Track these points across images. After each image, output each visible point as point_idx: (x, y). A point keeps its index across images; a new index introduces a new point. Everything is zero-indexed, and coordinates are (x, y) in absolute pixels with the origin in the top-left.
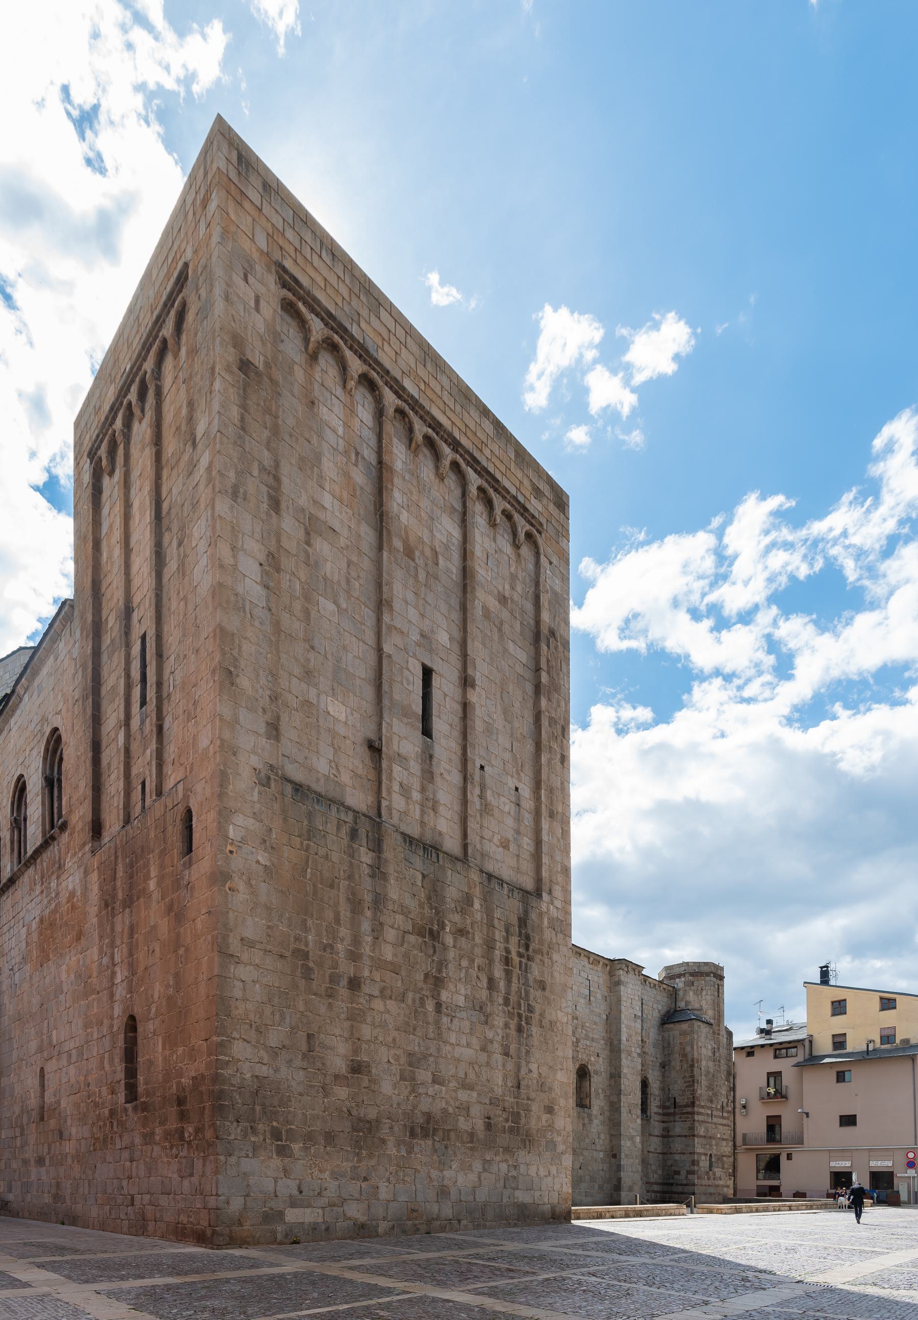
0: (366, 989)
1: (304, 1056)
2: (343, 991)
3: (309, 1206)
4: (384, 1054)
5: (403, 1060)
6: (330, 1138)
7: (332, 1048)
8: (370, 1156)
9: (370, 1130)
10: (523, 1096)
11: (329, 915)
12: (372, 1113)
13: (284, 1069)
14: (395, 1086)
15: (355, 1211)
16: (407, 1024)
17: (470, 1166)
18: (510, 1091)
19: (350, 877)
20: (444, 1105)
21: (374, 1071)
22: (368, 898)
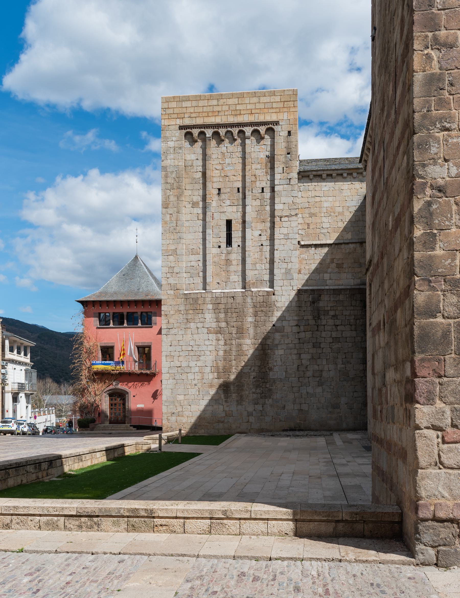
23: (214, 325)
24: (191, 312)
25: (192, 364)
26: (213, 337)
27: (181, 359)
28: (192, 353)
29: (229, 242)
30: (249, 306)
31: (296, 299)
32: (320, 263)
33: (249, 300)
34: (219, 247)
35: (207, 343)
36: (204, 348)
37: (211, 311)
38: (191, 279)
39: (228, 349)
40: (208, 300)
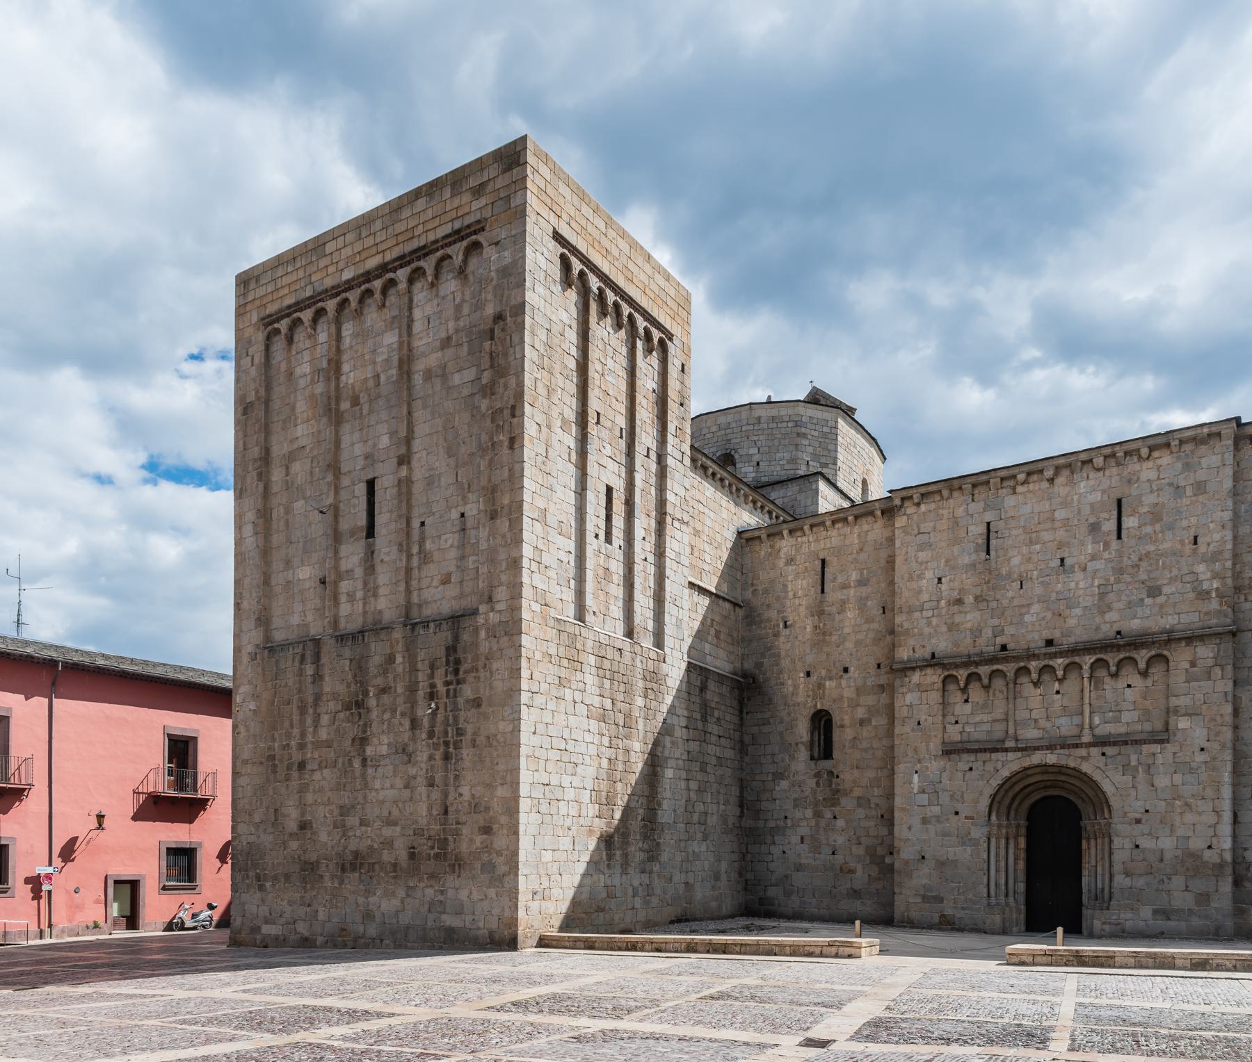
0: (309, 767)
1: (273, 824)
2: (295, 774)
3: (274, 923)
4: (321, 811)
5: (336, 812)
6: (287, 877)
7: (289, 816)
8: (313, 888)
9: (312, 869)
10: (450, 822)
11: (287, 724)
12: (313, 857)
13: (262, 835)
14: (329, 834)
15: (302, 928)
16: (338, 784)
17: (394, 892)
18: (435, 819)
19: (300, 691)
20: (369, 842)
21: (314, 826)
22: (310, 699)
23: (597, 701)
24: (565, 663)
25: (566, 781)
26: (594, 725)
27: (550, 767)
28: (566, 758)
29: (608, 539)
30: (639, 676)
31: (686, 680)
32: (702, 623)
33: (639, 664)
34: (597, 536)
35: (588, 738)
36: (582, 748)
37: (594, 670)
38: (558, 588)
39: (613, 757)
40: (590, 644)
